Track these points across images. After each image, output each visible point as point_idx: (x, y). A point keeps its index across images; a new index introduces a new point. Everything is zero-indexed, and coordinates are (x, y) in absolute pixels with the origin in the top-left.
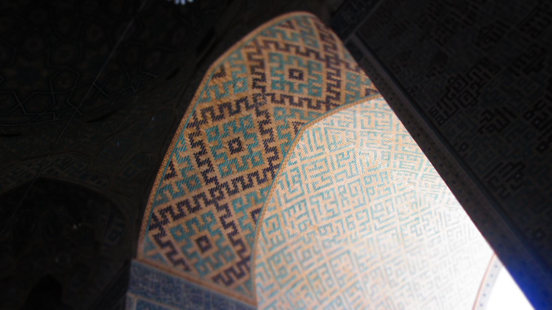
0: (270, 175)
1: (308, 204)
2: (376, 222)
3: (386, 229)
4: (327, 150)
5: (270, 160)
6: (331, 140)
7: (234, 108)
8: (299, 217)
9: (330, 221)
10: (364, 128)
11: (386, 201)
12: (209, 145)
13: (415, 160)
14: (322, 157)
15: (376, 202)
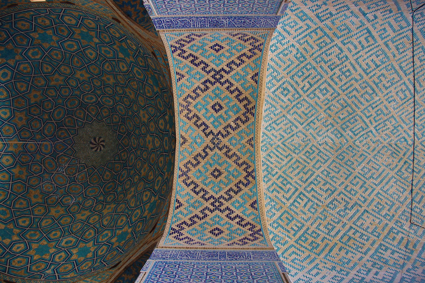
0: (251, 178)
1: (307, 194)
2: (371, 180)
3: (385, 181)
4: (294, 155)
5: (245, 170)
6: (293, 148)
7: (203, 154)
8: (305, 206)
9: (332, 197)
10: (303, 124)
11: (368, 163)
12: (198, 181)
13: (356, 121)
14: (294, 160)
15: (360, 168)
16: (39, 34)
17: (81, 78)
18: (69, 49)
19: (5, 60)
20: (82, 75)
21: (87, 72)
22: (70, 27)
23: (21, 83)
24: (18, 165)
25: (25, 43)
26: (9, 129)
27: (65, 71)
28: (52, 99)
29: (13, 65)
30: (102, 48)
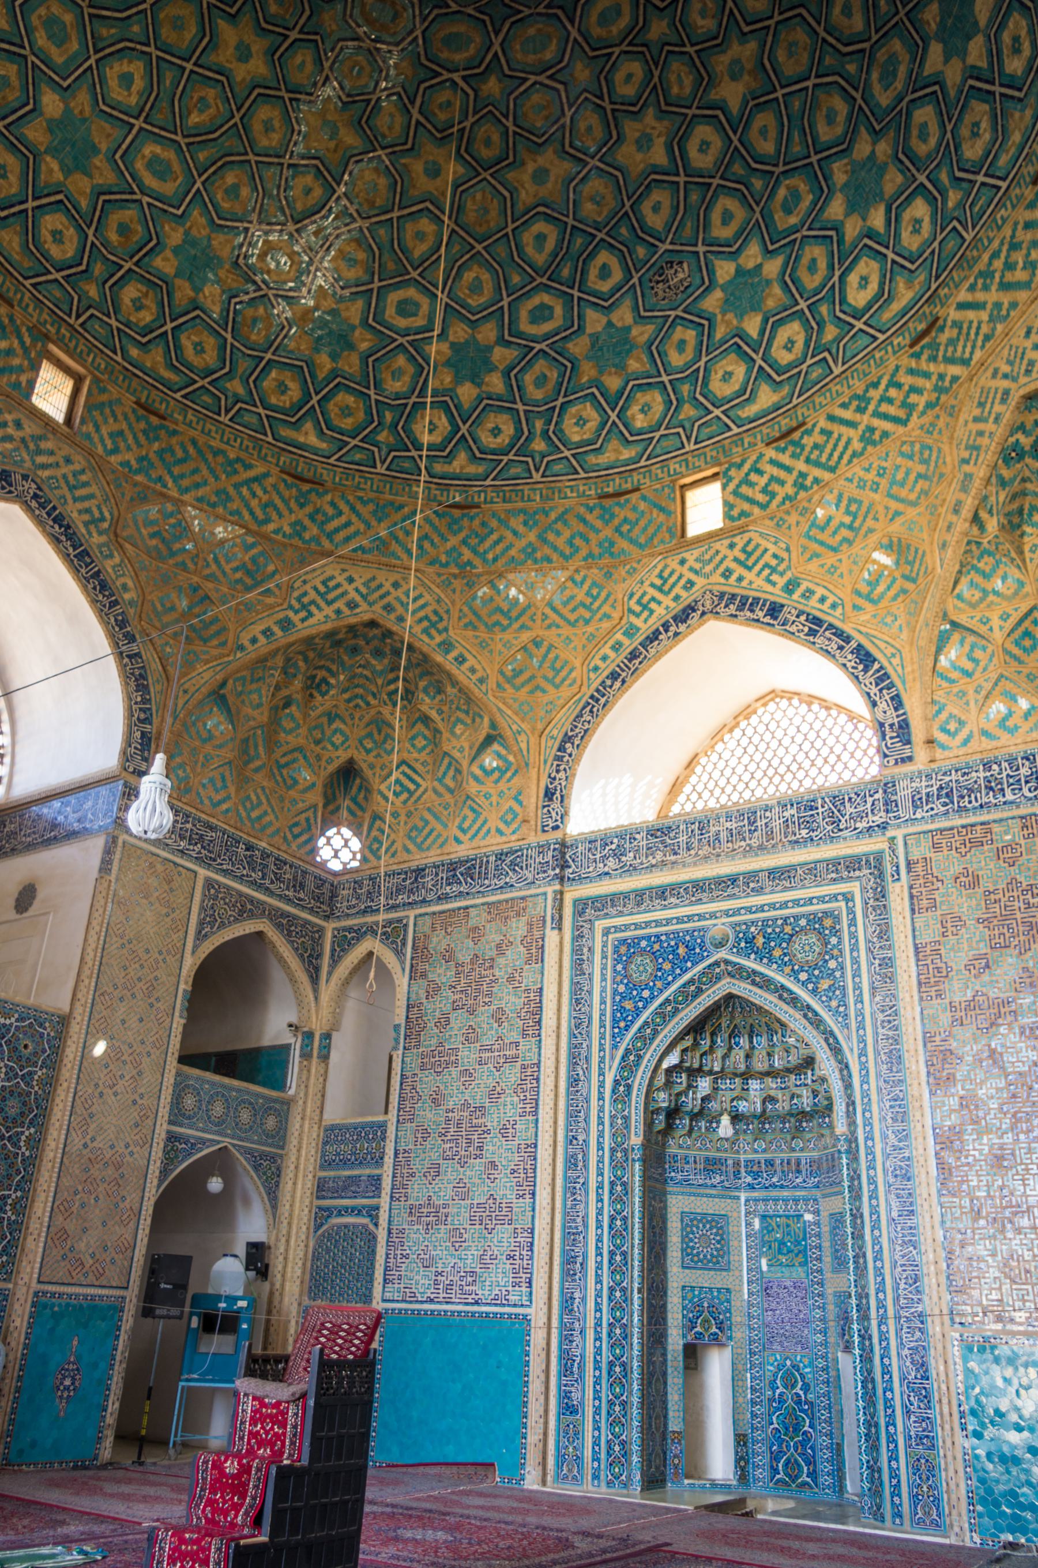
16: (197, 290)
17: (254, 48)
18: (176, 167)
19: (357, 333)
20: (244, 54)
21: (213, 44)
22: (81, 221)
23: (410, 244)
24: (713, 96)
25: (261, 311)
26: (592, 199)
27: (276, 124)
28: (412, 103)
29: (360, 304)
30: (58, 57)
